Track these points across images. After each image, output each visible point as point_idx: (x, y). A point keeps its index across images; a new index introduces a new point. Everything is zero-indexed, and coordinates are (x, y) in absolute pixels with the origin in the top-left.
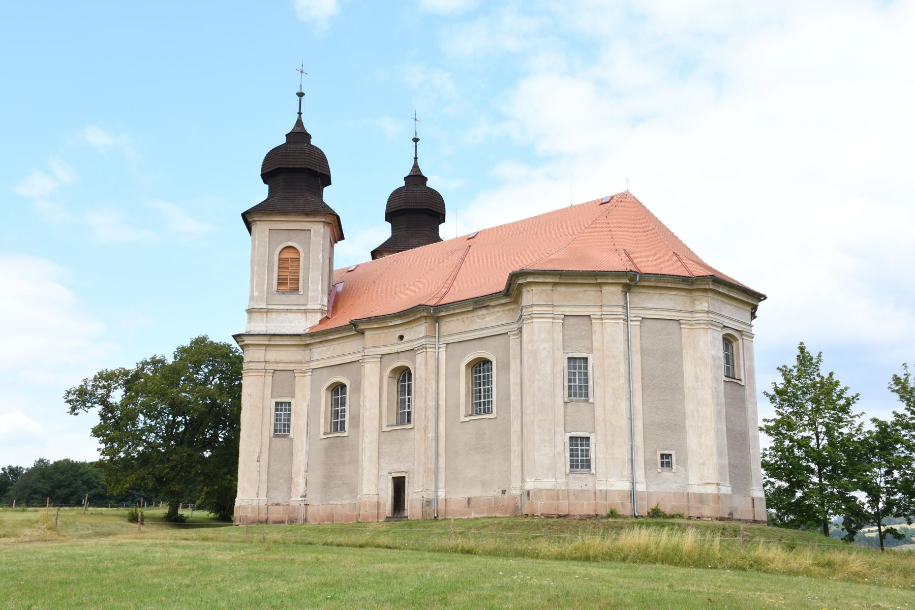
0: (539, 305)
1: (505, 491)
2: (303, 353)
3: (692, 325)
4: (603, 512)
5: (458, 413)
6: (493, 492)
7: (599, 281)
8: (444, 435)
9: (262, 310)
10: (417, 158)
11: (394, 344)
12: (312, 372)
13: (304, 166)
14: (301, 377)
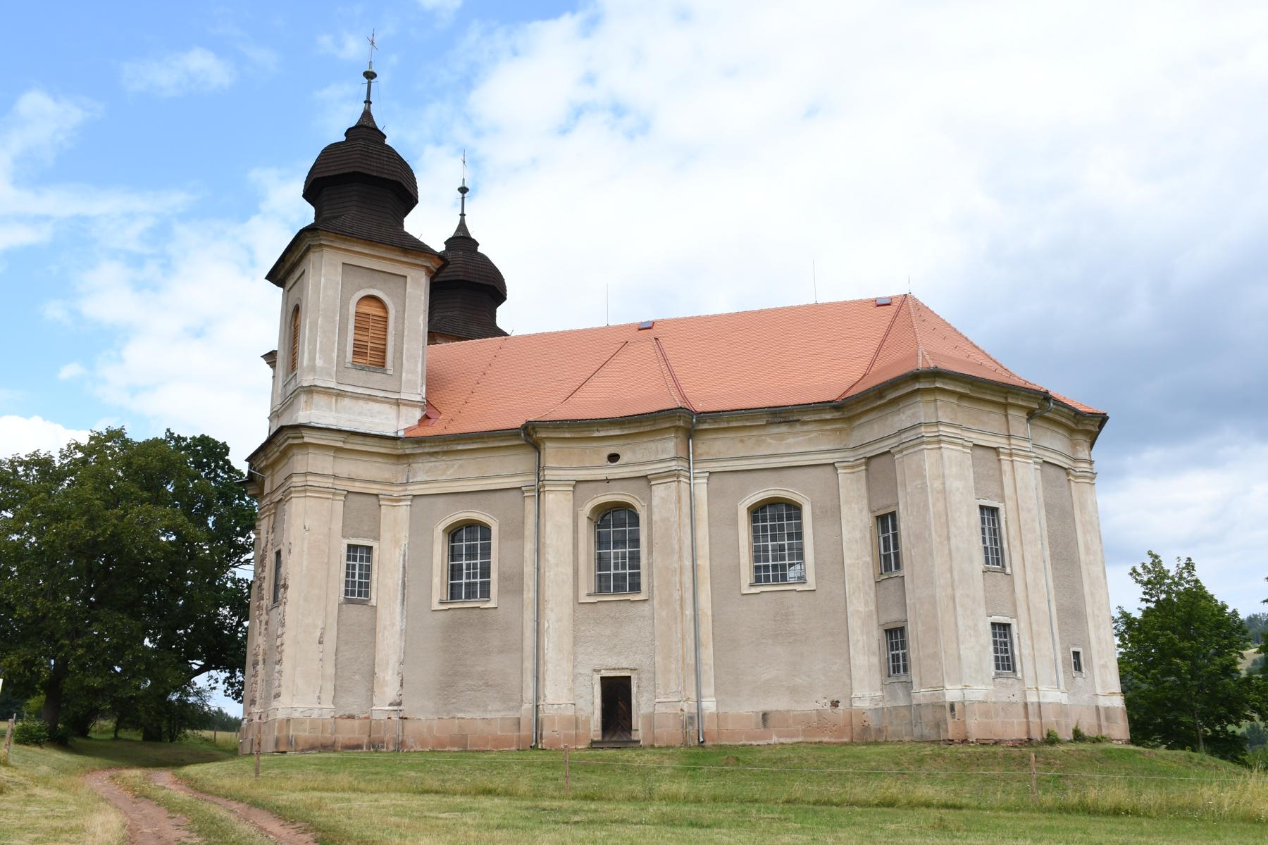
1: (838, 702)
2: (393, 467)
4: (1036, 735)
6: (814, 704)
7: (1010, 400)
8: (710, 613)
9: (331, 391)
10: (465, 215)
11: (600, 467)
12: (412, 500)
14: (390, 508)
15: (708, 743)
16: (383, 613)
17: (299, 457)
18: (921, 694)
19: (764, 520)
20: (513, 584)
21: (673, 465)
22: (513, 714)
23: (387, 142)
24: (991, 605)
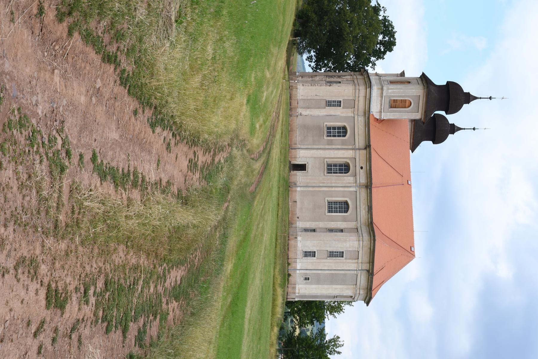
0: (363, 243)
2: (362, 111)
3: (355, 288)
4: (290, 261)
5: (329, 197)
6: (298, 213)
7: (371, 263)
13: (450, 108)
15: (290, 188)
16: (324, 110)
17: (364, 87)
18: (299, 233)
19: (344, 205)
20: (330, 143)
21: (358, 182)
22: (298, 143)
23: (465, 105)
24: (319, 251)
